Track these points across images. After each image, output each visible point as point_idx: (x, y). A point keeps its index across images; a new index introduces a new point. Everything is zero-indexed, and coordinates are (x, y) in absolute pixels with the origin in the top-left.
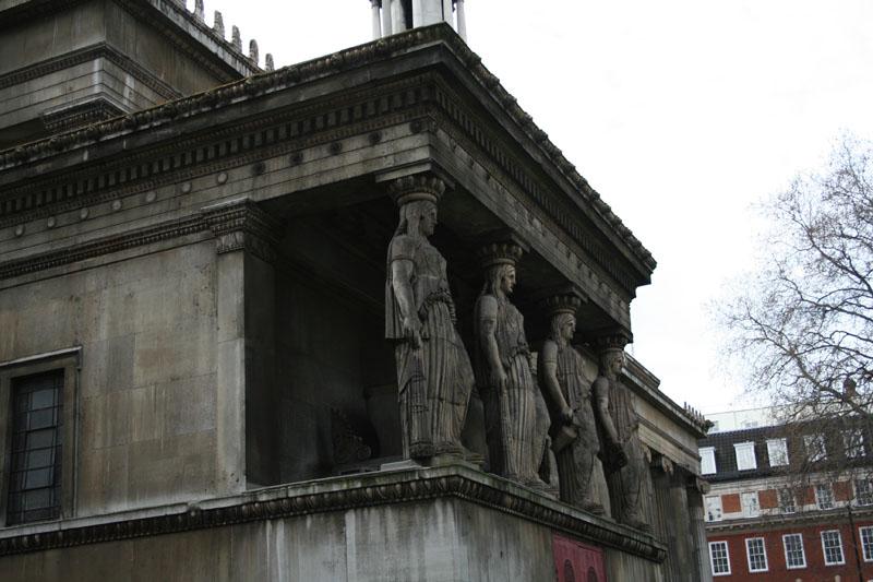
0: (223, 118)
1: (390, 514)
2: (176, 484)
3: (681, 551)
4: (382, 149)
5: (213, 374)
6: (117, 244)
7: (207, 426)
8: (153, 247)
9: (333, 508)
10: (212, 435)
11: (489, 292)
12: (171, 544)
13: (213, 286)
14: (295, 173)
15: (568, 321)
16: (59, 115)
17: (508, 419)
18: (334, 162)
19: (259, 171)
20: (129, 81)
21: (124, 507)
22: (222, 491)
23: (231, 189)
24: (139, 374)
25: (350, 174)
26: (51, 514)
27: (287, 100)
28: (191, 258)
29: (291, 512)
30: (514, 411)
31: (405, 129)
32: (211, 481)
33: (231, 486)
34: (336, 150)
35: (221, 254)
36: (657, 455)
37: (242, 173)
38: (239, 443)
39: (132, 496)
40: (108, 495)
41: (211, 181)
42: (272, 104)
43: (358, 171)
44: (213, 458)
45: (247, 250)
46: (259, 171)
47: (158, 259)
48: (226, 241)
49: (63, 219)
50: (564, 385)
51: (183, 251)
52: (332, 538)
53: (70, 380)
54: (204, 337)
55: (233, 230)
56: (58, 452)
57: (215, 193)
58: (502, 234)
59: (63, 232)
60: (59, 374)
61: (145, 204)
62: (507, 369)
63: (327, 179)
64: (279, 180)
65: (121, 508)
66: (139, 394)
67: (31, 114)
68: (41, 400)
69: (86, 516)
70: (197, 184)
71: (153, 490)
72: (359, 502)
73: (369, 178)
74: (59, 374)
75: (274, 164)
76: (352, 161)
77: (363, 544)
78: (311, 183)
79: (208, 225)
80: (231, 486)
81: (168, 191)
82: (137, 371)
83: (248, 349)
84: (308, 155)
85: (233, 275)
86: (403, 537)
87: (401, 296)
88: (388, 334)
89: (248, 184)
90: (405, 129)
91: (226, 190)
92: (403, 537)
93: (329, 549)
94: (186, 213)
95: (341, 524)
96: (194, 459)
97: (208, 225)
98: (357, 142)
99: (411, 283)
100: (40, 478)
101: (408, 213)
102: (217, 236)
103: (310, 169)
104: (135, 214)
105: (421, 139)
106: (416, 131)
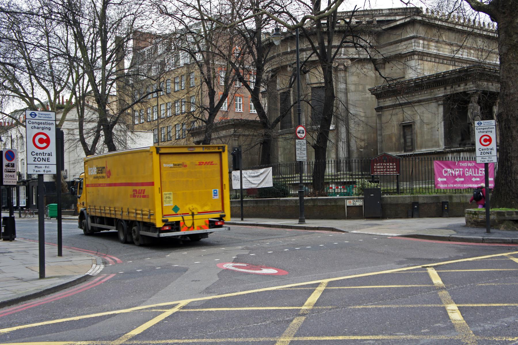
0: (438, 79)
1: (468, 153)
2: (433, 146)
4: (467, 87)
6: (419, 101)
10: (439, 138)
12: (432, 156)
13: (438, 111)
14: (452, 90)
16: (405, 54)
18: (459, 88)
19: (445, 89)
20: (421, 42)
21: (424, 150)
22: (440, 148)
23: (440, 93)
25: (462, 91)
26: (411, 151)
27: (449, 77)
28: (433, 105)
31: (471, 83)
32: (439, 146)
33: (442, 147)
34: (459, 86)
35: (439, 105)
37: (442, 89)
38: (443, 140)
39: (425, 148)
40: (421, 147)
41: (437, 90)
42: (447, 78)
44: (439, 142)
45: (444, 105)
46: (445, 89)
47: (427, 105)
48: (440, 102)
49: (410, 95)
53: (413, 127)
55: (440, 101)
56: (412, 139)
57: (437, 92)
59: (410, 98)
60: (411, 125)
61: (424, 93)
64: (449, 91)
65: (424, 151)
67: (398, 52)
68: (408, 132)
69: (417, 152)
70: (434, 90)
71: (429, 147)
73: (465, 92)
74: (411, 125)
75: (448, 88)
79: (437, 99)
80: (442, 147)
81: (429, 91)
83: (444, 123)
85: (441, 109)
89: (443, 91)
90: (471, 83)
91: (440, 92)
94: (432, 96)
96: (436, 142)
97: (437, 99)
99: (472, 113)
100: (409, 144)
101: (472, 99)
102: (438, 101)
104: (423, 95)
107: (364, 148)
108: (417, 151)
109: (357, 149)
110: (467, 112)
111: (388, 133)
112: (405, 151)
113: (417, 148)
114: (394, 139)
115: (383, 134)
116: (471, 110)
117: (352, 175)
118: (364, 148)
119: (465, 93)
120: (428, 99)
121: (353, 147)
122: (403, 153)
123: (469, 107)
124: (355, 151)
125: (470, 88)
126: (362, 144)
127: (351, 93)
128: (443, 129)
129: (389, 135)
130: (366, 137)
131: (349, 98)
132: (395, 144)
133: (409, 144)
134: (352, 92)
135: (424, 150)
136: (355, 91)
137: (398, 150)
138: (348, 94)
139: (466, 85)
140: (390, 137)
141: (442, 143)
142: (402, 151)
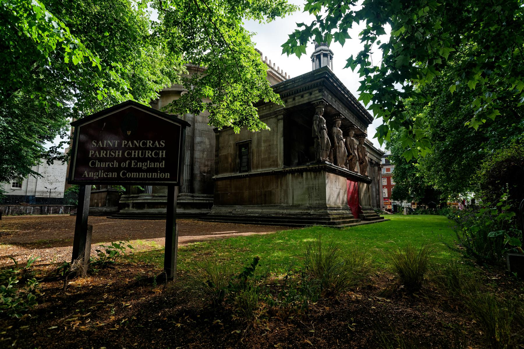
1: (312, 173)
2: (270, 166)
3: (376, 180)
4: (312, 96)
5: (277, 144)
7: (276, 155)
8: (265, 119)
9: (301, 172)
10: (277, 156)
11: (335, 126)
14: (294, 102)
15: (352, 133)
17: (338, 154)
18: (302, 99)
21: (260, 170)
24: (263, 144)
25: (305, 102)
29: (292, 172)
30: (339, 152)
32: (277, 165)
33: (281, 167)
36: (371, 160)
38: (282, 158)
39: (262, 168)
40: (257, 167)
43: (307, 101)
44: (277, 161)
50: (351, 146)
51: (271, 119)
52: (301, 177)
54: (275, 137)
55: (281, 115)
56: (248, 159)
58: (338, 114)
61: (263, 110)
62: (338, 143)
63: (300, 103)
65: (260, 171)
66: (263, 148)
69: (253, 172)
71: (266, 167)
72: (306, 170)
74: (248, 144)
76: (306, 99)
77: (307, 179)
78: (297, 104)
82: (263, 144)
83: (284, 139)
84: (296, 98)
85: (281, 124)
86: (315, 178)
87: (316, 128)
88: (313, 136)
92: (315, 178)
93: (300, 180)
95: (302, 175)
96: (274, 161)
98: (307, 95)
100: (244, 164)
102: (277, 116)
103: (297, 101)
105: (320, 94)
106: (319, 92)
107: (207, 173)
108: (252, 171)
109: (201, 173)
110: (312, 124)
111: (224, 154)
112: (240, 172)
113: (253, 168)
114: (230, 160)
115: (220, 155)
116: (318, 122)
117: (193, 196)
118: (207, 173)
119: (309, 104)
120: (267, 114)
121: (197, 172)
122: (238, 174)
123: (314, 118)
124: (199, 175)
125: (316, 97)
126: (206, 169)
127: (198, 124)
128: (282, 146)
129: (225, 155)
130: (209, 163)
131: (196, 128)
132: (231, 164)
133: (244, 164)
134: (199, 122)
135: (260, 170)
136: (202, 122)
137: (233, 170)
138: (196, 124)
139: (311, 94)
140: (226, 157)
141: (280, 161)
142: (237, 171)
